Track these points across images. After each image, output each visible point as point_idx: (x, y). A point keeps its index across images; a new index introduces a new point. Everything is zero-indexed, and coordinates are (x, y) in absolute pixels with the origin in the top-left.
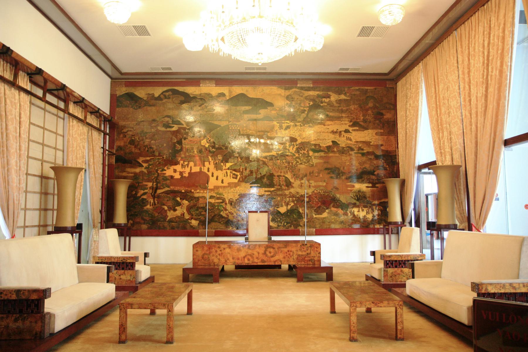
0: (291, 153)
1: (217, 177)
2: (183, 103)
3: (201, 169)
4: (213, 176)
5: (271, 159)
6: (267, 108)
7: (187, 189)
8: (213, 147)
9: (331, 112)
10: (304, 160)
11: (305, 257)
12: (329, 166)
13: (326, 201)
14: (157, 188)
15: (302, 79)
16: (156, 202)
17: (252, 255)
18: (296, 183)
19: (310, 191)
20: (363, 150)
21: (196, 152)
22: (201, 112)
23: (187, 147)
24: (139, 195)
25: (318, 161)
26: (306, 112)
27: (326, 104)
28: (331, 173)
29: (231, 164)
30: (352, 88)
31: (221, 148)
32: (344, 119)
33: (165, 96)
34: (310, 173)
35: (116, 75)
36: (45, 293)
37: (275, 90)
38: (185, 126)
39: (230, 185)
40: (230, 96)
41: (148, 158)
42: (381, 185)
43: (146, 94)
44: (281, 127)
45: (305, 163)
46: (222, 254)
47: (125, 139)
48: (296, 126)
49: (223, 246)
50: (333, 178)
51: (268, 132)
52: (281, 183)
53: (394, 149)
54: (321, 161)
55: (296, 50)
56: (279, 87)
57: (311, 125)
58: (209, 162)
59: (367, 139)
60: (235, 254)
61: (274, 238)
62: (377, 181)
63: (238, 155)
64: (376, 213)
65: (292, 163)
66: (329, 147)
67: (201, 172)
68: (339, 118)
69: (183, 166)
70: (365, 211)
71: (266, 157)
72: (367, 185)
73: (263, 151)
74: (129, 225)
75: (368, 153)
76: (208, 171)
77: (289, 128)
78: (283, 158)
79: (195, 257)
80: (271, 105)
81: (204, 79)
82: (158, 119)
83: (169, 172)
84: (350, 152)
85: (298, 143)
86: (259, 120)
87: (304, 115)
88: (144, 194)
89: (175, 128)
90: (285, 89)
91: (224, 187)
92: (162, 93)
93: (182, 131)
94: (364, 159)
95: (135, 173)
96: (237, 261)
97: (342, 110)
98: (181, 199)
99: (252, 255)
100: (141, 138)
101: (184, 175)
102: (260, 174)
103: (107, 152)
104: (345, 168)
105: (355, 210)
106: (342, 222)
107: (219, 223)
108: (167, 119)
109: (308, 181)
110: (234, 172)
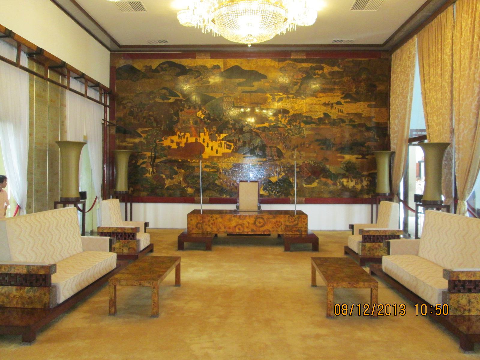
0: (283, 125)
1: (212, 148)
2: (179, 75)
3: (196, 139)
4: (208, 146)
5: (264, 131)
6: (260, 80)
7: (183, 158)
8: (208, 118)
10: (296, 132)
11: (293, 228)
12: (320, 138)
13: (317, 172)
15: (297, 52)
16: (155, 170)
17: (242, 225)
18: (287, 154)
19: (301, 162)
20: (354, 122)
21: (191, 124)
22: (196, 84)
23: (183, 118)
24: (139, 164)
29: (225, 135)
30: (346, 60)
32: (336, 91)
34: (301, 145)
35: (115, 47)
36: (51, 269)
37: (269, 62)
38: (181, 98)
39: (225, 155)
40: (224, 68)
41: (147, 129)
43: (144, 67)
45: (296, 134)
46: (214, 223)
47: (125, 110)
48: (288, 98)
49: (215, 216)
50: (324, 150)
51: (261, 104)
52: (273, 154)
53: (385, 121)
55: (287, 29)
56: (273, 59)
57: (303, 97)
59: (359, 111)
61: (265, 207)
63: (231, 127)
64: (365, 183)
65: (284, 135)
66: (320, 120)
67: (196, 142)
68: (331, 90)
69: (180, 137)
70: (354, 181)
71: (258, 129)
73: (257, 123)
74: (130, 192)
75: (360, 125)
76: (204, 141)
77: (282, 100)
79: (190, 226)
80: (264, 77)
81: (200, 51)
82: (155, 91)
83: (166, 142)
84: (342, 124)
86: (252, 92)
87: (297, 87)
88: (143, 163)
89: (172, 100)
91: (219, 158)
92: (159, 66)
93: (179, 103)
94: (355, 130)
95: (134, 143)
98: (178, 168)
99: (242, 225)
100: (139, 110)
101: (181, 145)
102: (253, 145)
103: (108, 123)
105: (345, 181)
106: (330, 192)
107: (214, 191)
109: (299, 152)
110: (228, 143)
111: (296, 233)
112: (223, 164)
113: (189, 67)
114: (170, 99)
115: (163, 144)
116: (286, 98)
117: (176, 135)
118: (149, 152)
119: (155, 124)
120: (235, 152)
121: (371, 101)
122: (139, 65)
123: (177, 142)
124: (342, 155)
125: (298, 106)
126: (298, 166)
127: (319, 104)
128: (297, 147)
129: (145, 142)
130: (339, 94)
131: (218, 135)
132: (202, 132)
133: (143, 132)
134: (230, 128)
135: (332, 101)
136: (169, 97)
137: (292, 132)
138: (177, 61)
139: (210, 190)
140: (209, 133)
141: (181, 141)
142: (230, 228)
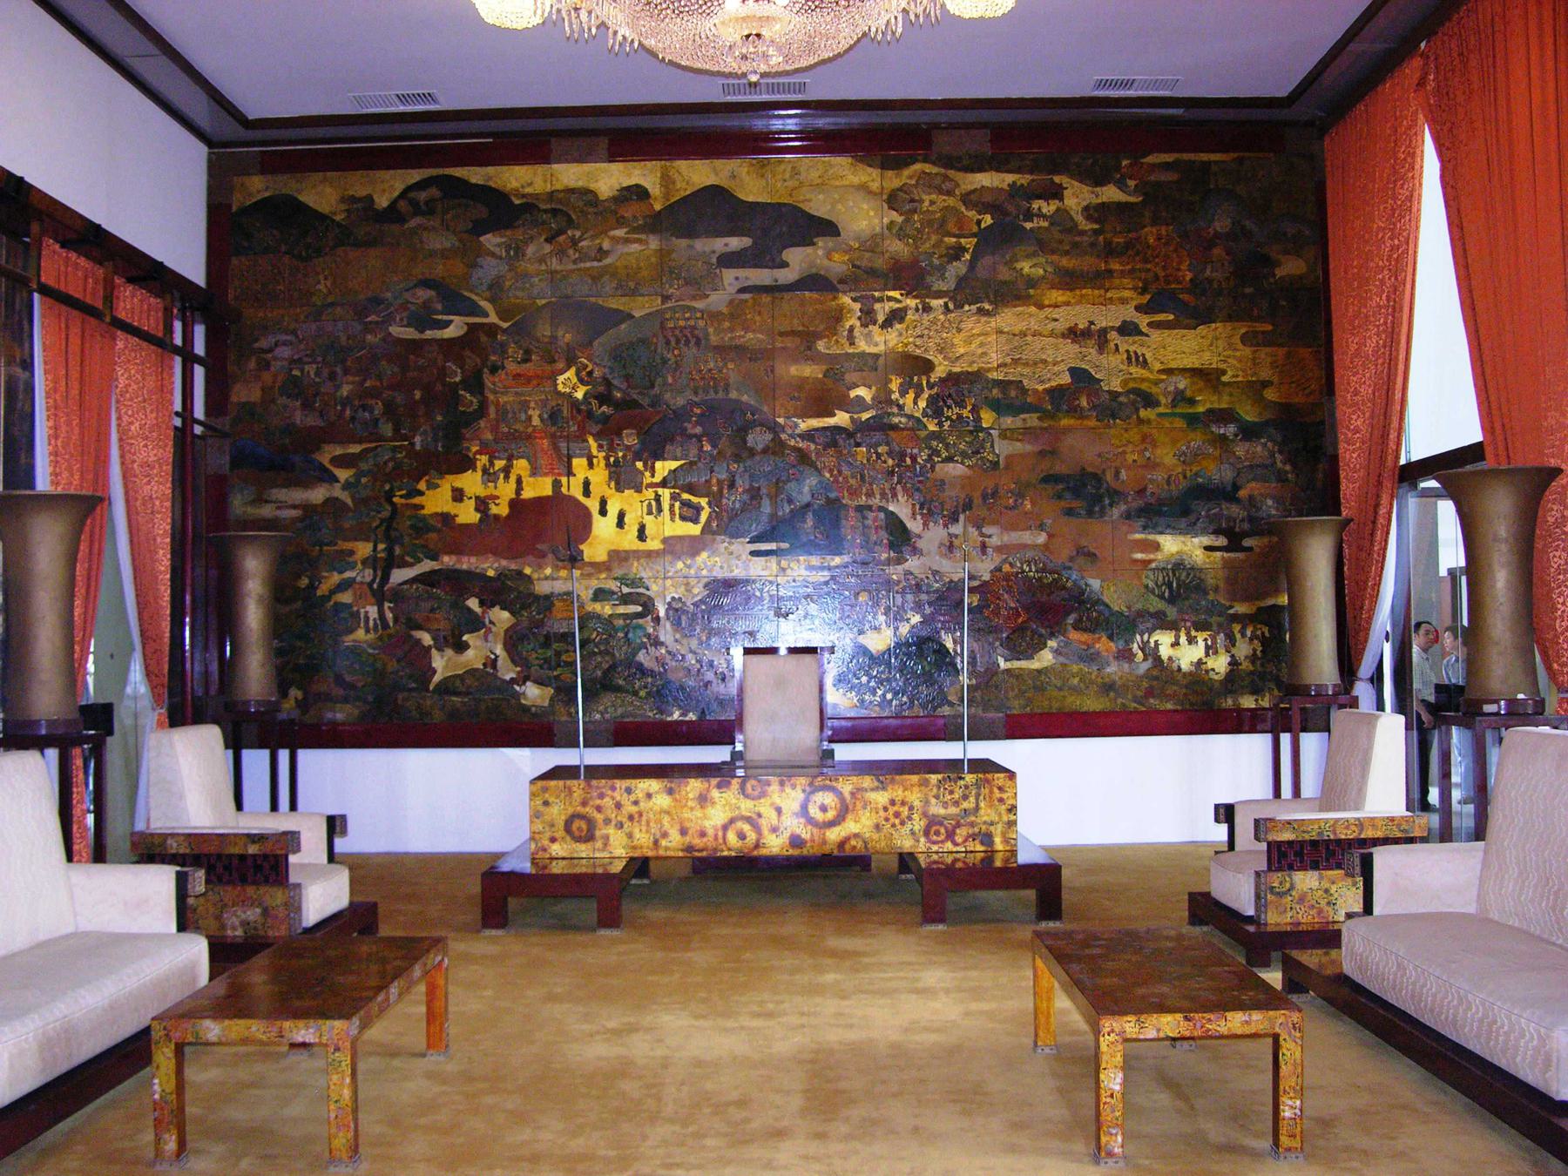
0: (910, 417)
1: (621, 516)
3: (557, 485)
4: (603, 512)
7: (504, 563)
8: (604, 399)
9: (1067, 253)
12: (1061, 468)
14: (391, 563)
15: (952, 126)
16: (389, 616)
19: (985, 568)
20: (1192, 402)
21: (536, 421)
24: (323, 589)
25: (1018, 447)
26: (968, 257)
27: (1046, 224)
28: (1067, 495)
29: (674, 465)
30: (1150, 159)
31: (634, 404)
32: (1117, 282)
33: (414, 204)
34: (984, 497)
35: (232, 130)
38: (493, 318)
39: (673, 546)
40: (666, 196)
41: (355, 449)
42: (1266, 540)
44: (868, 317)
45: (964, 455)
46: (641, 815)
54: (1029, 448)
57: (987, 306)
58: (590, 459)
59: (1208, 359)
60: (687, 814)
62: (1246, 526)
63: (698, 430)
64: (1243, 649)
65: (914, 459)
66: (1057, 393)
68: (1099, 279)
69: (489, 476)
70: (1201, 644)
72: (1206, 540)
76: (587, 493)
77: (902, 320)
78: (878, 436)
80: (828, 228)
82: (389, 295)
83: (436, 501)
84: (1143, 413)
85: (934, 377)
87: (958, 268)
89: (455, 328)
90: (884, 166)
91: (649, 554)
93: (484, 338)
94: (1197, 440)
95: (308, 508)
96: (698, 842)
97: (1108, 243)
98: (482, 604)
100: (325, 372)
101: (494, 510)
102: (790, 501)
103: (198, 430)
104: (1123, 474)
105: (1164, 640)
106: (1108, 688)
107: (636, 693)
108: (424, 294)
110: (685, 496)
111: (971, 846)
112: (668, 583)
113: (524, 196)
114: (448, 324)
115: (423, 507)
116: (917, 310)
117: (475, 470)
118: (367, 540)
119: (387, 429)
120: (714, 533)
121: (1259, 319)
122: (322, 195)
123: (477, 498)
124: (1151, 537)
125: (968, 342)
126: (976, 583)
127: (1052, 334)
128: (968, 506)
129: (349, 501)
130: (1127, 294)
131: (645, 465)
132: (581, 456)
133: (342, 461)
134: (691, 437)
135: (1102, 323)
136: (445, 317)
137: (947, 446)
138: (475, 175)
139: (618, 689)
140: (607, 458)
141: (496, 493)
142: (703, 834)
